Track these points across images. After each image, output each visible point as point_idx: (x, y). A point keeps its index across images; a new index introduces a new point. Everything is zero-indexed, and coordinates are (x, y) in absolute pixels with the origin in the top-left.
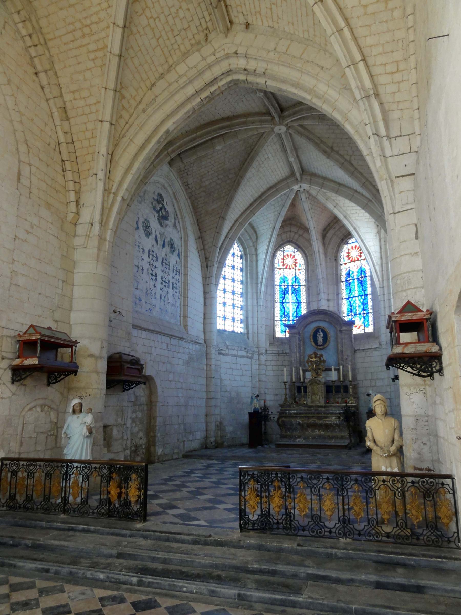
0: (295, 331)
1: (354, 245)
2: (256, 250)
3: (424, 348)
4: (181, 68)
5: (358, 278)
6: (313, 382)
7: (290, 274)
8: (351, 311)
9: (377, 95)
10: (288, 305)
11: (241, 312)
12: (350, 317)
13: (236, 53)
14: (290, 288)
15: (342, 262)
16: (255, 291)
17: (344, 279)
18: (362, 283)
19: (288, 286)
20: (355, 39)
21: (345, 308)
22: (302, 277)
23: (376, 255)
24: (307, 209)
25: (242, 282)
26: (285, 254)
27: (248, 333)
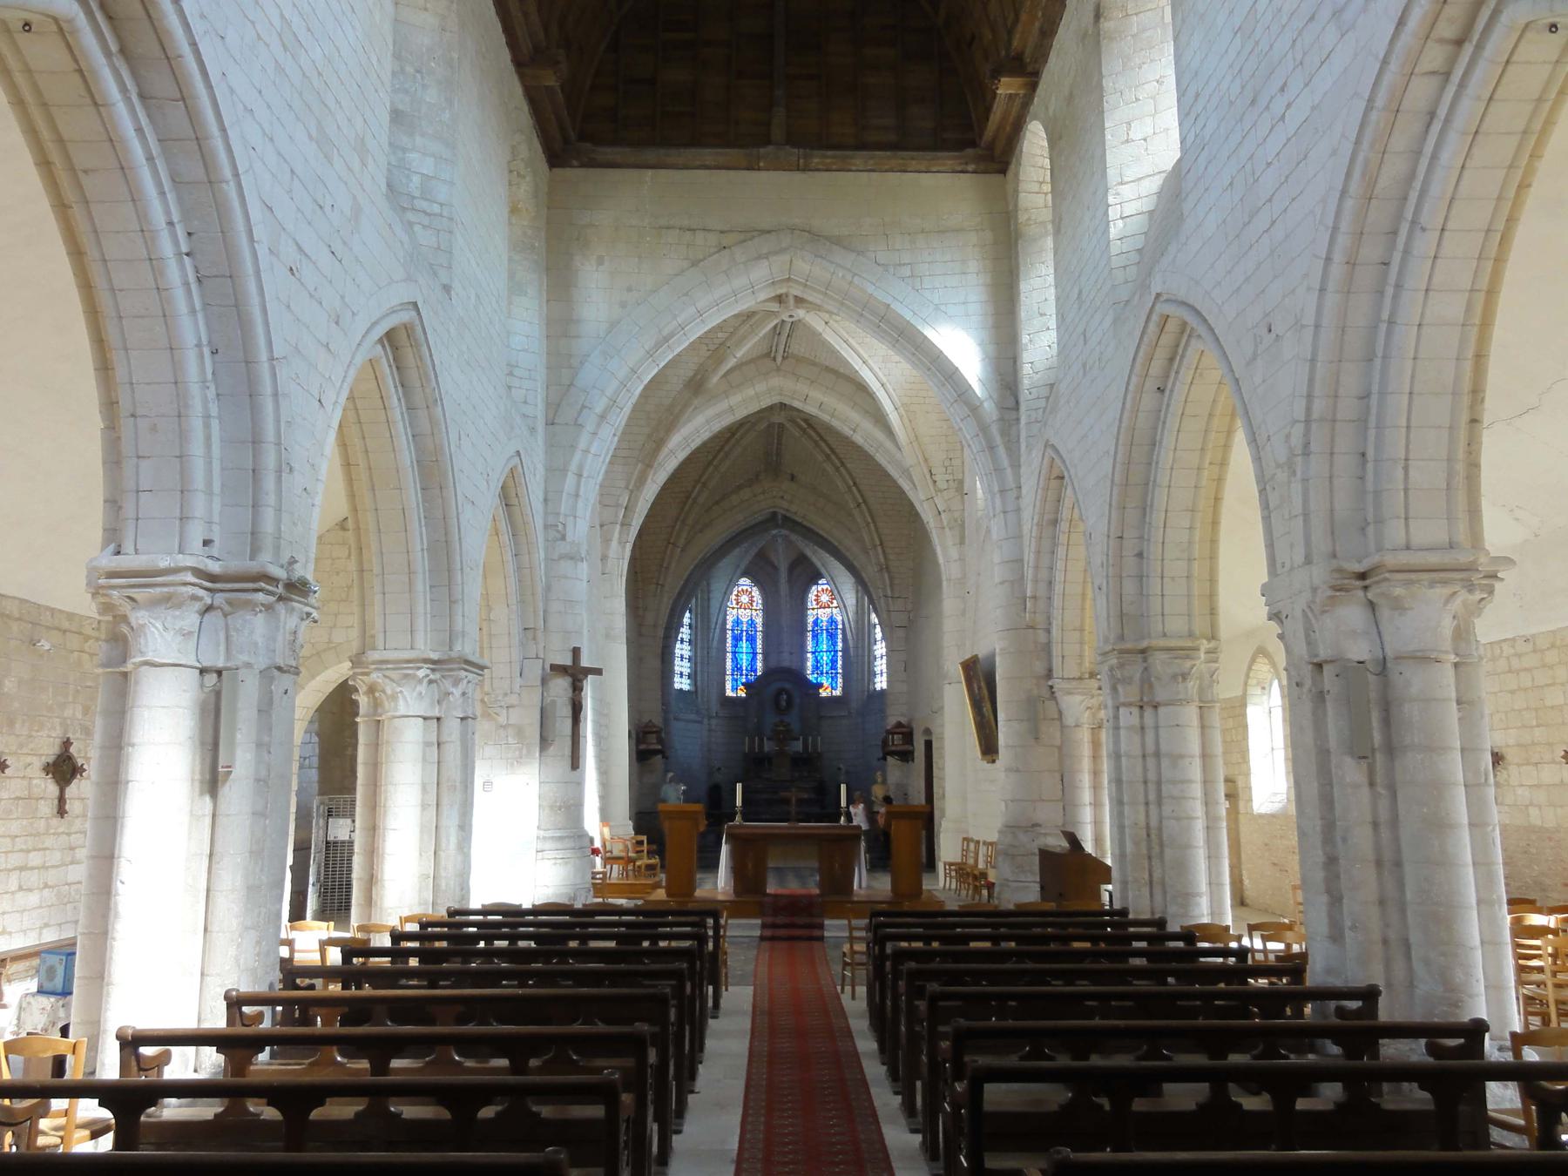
1: (825, 587)
2: (708, 585)
3: (906, 747)
4: (735, 499)
7: (745, 615)
8: (817, 668)
9: (887, 568)
11: (689, 665)
13: (782, 497)
14: (744, 634)
17: (810, 628)
18: (832, 636)
19: (742, 631)
21: (809, 664)
22: (759, 621)
25: (690, 625)
27: (696, 691)
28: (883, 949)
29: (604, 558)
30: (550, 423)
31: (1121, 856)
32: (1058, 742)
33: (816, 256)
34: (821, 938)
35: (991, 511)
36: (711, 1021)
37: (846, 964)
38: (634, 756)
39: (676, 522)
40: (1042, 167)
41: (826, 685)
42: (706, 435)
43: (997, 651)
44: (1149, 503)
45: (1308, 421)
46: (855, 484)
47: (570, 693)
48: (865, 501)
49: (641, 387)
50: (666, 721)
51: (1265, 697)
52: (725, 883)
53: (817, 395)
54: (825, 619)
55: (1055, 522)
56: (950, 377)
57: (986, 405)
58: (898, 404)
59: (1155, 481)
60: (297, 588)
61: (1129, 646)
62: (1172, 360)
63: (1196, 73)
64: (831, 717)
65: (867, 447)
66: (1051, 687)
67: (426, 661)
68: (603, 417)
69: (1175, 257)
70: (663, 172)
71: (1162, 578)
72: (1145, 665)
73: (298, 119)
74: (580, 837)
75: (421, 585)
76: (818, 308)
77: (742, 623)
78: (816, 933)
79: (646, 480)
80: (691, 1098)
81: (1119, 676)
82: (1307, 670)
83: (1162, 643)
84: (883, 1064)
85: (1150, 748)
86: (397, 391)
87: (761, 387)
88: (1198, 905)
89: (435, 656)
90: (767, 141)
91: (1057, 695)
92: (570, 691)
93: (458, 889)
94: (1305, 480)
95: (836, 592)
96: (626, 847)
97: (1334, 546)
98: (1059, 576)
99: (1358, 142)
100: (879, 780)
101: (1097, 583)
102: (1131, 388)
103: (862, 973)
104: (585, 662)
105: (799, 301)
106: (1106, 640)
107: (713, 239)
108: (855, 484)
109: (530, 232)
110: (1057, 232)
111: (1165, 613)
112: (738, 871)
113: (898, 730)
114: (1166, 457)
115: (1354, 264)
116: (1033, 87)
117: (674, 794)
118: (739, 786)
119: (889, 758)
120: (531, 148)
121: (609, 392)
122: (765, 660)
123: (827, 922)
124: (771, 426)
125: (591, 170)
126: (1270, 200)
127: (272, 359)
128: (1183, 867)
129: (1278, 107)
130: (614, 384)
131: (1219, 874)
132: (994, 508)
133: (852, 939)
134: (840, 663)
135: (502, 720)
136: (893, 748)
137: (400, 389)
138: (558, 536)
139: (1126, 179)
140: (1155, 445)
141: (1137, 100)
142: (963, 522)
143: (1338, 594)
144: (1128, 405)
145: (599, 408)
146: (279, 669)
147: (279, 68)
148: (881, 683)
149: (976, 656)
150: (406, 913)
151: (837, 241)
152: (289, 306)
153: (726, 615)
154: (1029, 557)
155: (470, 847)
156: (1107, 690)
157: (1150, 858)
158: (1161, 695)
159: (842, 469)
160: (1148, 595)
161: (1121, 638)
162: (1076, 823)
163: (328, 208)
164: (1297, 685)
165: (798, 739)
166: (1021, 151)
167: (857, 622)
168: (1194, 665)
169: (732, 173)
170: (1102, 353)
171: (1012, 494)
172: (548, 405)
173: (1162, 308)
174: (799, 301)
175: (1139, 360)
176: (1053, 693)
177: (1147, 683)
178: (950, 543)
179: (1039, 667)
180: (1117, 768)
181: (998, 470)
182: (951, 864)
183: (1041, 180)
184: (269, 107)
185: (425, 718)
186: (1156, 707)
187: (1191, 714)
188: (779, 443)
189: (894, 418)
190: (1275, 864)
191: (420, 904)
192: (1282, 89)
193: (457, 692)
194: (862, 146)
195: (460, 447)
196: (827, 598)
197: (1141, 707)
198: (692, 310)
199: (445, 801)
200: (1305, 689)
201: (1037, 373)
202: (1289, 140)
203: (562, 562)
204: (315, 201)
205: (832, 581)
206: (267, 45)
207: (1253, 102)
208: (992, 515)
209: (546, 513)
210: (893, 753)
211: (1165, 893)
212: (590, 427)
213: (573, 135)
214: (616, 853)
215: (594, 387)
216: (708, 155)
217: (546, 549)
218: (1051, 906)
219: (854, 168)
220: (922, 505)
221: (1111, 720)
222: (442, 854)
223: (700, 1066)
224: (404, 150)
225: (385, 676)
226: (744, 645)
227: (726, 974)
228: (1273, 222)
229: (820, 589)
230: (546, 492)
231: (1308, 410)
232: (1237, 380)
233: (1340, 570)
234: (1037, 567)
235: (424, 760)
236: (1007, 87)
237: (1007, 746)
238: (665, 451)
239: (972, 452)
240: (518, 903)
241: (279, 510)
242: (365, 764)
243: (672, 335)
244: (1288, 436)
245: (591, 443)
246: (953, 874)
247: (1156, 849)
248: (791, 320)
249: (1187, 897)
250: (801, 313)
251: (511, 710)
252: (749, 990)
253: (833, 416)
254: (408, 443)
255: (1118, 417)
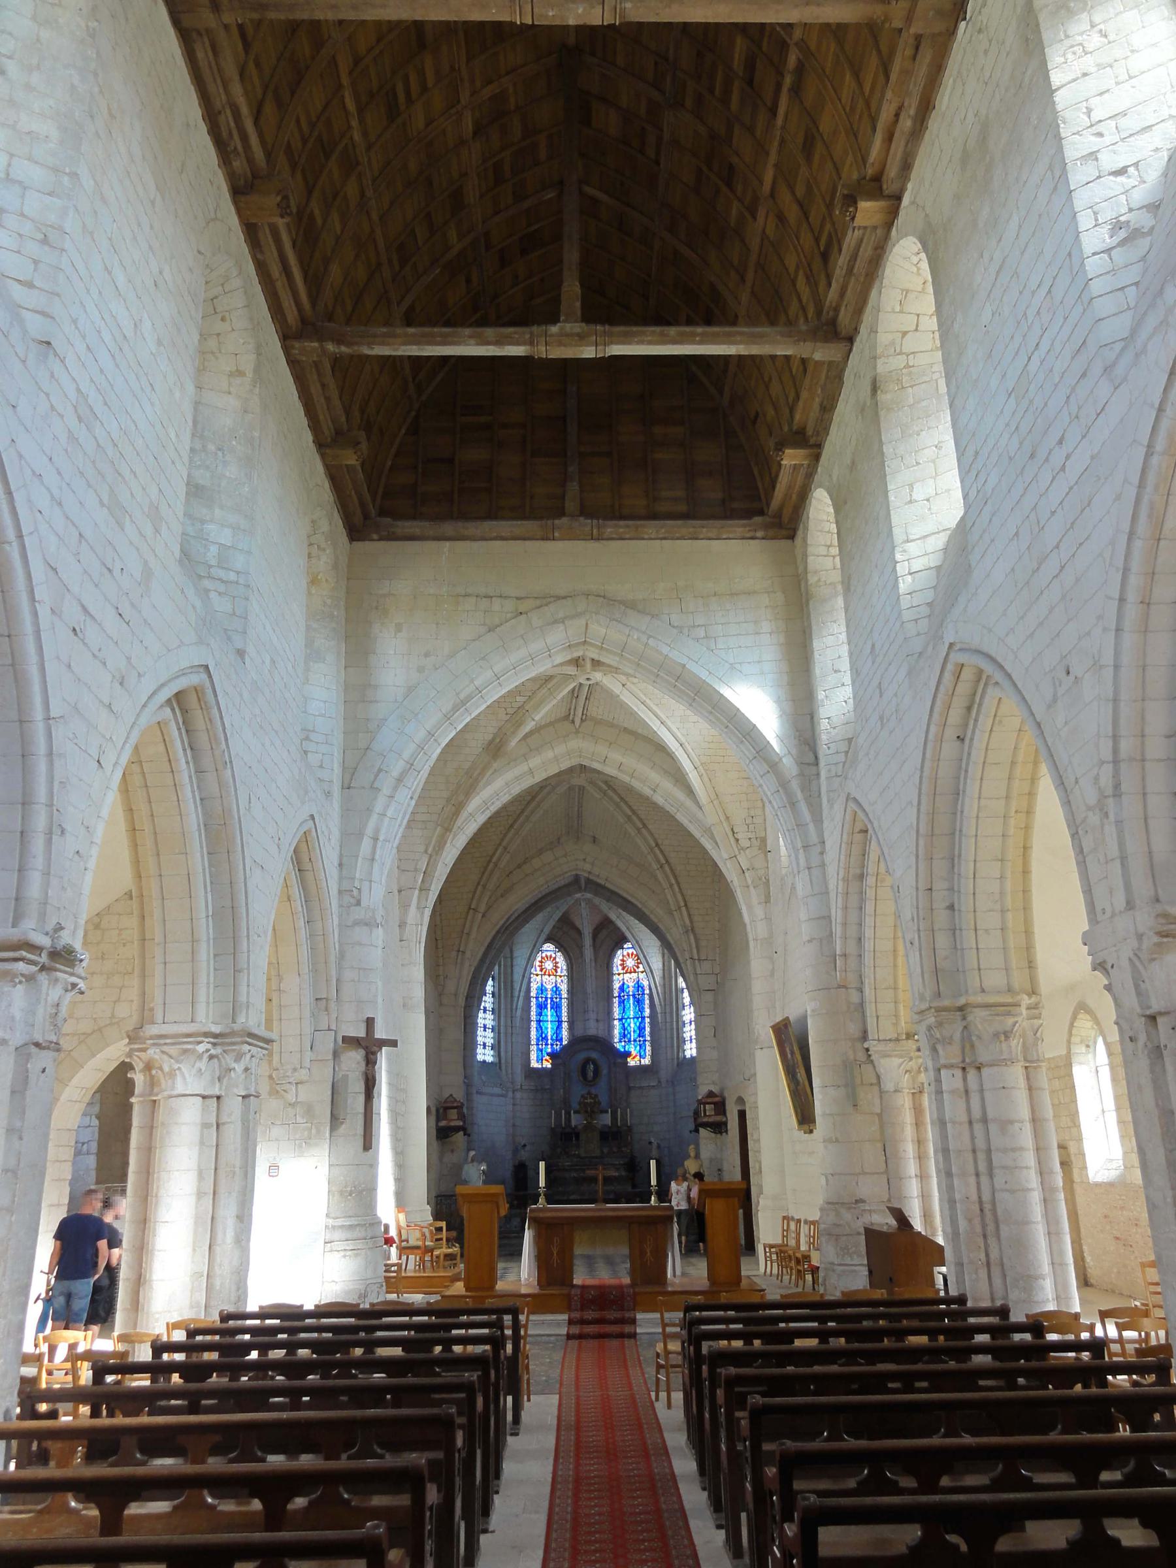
0: (560, 1061)
1: (630, 951)
2: (512, 951)
3: (719, 1118)
4: (536, 863)
5: (634, 995)
6: (589, 1127)
7: (549, 982)
8: (625, 1036)
9: (692, 929)
10: (545, 1024)
11: (492, 1035)
12: (623, 1044)
13: (584, 860)
14: (549, 1001)
15: (615, 971)
16: (509, 1006)
17: (616, 994)
18: (639, 1002)
19: (546, 998)
20: (680, 889)
21: (617, 1032)
22: (564, 987)
23: (658, 974)
24: (584, 915)
25: (493, 994)
26: (544, 955)
28: (698, 1349)
29: (403, 925)
30: (346, 787)
31: (954, 1235)
32: (879, 1111)
33: (612, 620)
34: (633, 1335)
35: (795, 866)
36: (510, 1439)
37: (659, 1366)
38: (434, 1132)
39: (477, 888)
40: (829, 532)
41: (634, 1053)
42: (505, 798)
43: (809, 1013)
44: (956, 853)
45: (1116, 762)
46: (657, 845)
47: (362, 1066)
48: (667, 861)
49: (439, 751)
50: (468, 1095)
51: (1090, 1056)
52: (529, 1274)
53: (616, 756)
54: (631, 984)
55: (861, 877)
56: (748, 734)
57: (784, 760)
58: (698, 764)
59: (961, 831)
60: (62, 956)
61: (946, 1003)
62: (969, 709)
63: (974, 435)
64: (640, 1088)
65: (668, 807)
66: (867, 1050)
67: (206, 1034)
68: (400, 780)
69: (967, 606)
70: (460, 545)
71: (976, 930)
72: (964, 1023)
73: (89, 486)
74: (372, 1225)
75: (204, 953)
76: (616, 670)
77: (546, 990)
78: (627, 1329)
79: (445, 844)
80: (483, 1538)
81: (938, 1036)
82: (1140, 1024)
83: (980, 999)
84: (704, 1489)
85: (977, 1113)
86: (186, 755)
87: (560, 749)
88: (1043, 1288)
89: (216, 1029)
90: (561, 513)
91: (873, 1058)
92: (363, 1064)
93: (234, 1288)
94: (1119, 823)
95: (641, 956)
96: (424, 1235)
97: (1156, 891)
98: (869, 933)
99: (1141, 485)
100: (692, 1154)
101: (908, 937)
102: (931, 736)
103: (678, 1379)
104: (380, 1034)
105: (596, 663)
106: (922, 998)
107: (509, 605)
108: (657, 845)
109: (329, 601)
110: (847, 589)
111: (981, 967)
112: (542, 1259)
113: (709, 1100)
114: (970, 806)
115: (1149, 604)
116: (817, 457)
117: (475, 1174)
118: (542, 1165)
119: (701, 1130)
120: (331, 522)
121: (406, 755)
122: (571, 1028)
123: (639, 1316)
124: (571, 788)
125: (389, 542)
126: (1057, 547)
127: (48, 718)
128: (1022, 1245)
129: (1058, 458)
130: (412, 747)
131: (1062, 1253)
132: (798, 864)
133: (666, 1337)
134: (648, 1029)
135: (291, 1097)
136: (705, 1120)
137: (189, 751)
138: (353, 901)
139: (911, 537)
140: (958, 794)
141: (918, 464)
142: (768, 881)
143: (1165, 940)
144: (928, 755)
145: (396, 769)
146: (37, 1045)
147: (72, 438)
148: (690, 1050)
149: (788, 1018)
150: (175, 1318)
151: (631, 605)
152: (69, 666)
153: (529, 982)
154: (837, 914)
155: (248, 1240)
156: (926, 1051)
157: (985, 1236)
158: (983, 1056)
159: (644, 831)
160: (963, 949)
161: (939, 995)
162: (902, 1198)
163: (117, 572)
164: (1131, 1039)
165: (607, 1112)
166: (808, 518)
167: (664, 985)
168: (1016, 1022)
169: (528, 543)
170: (898, 705)
171: (818, 849)
172: (344, 769)
173: (957, 657)
174: (596, 663)
175: (937, 710)
176: (870, 1056)
177: (968, 1042)
178: (755, 900)
179: (853, 1029)
180: (943, 1136)
181: (800, 825)
182: (771, 1246)
183: (829, 543)
184: (59, 473)
185: (204, 1097)
186: (979, 1069)
187: (1016, 1074)
188: (580, 806)
189: (693, 777)
190: (1117, 1238)
191: (192, 1307)
192: (1060, 442)
193: (239, 1067)
194: (654, 516)
195: (249, 810)
196: (633, 963)
197: (964, 1069)
198: (489, 674)
199: (222, 1190)
200: (1141, 1043)
201: (834, 728)
202: (1071, 488)
203: (357, 929)
204: (104, 564)
205: (638, 945)
206: (62, 416)
207: (1032, 456)
208: (796, 872)
209: (341, 878)
210: (705, 1125)
211: (1004, 1276)
212: (386, 791)
213: (373, 513)
214: (412, 1242)
215: (391, 750)
216: (504, 526)
217: (340, 916)
218: (880, 1294)
219: (646, 536)
220: (725, 864)
221: (933, 1084)
222: (218, 1250)
223: (495, 1497)
224: (203, 522)
225: (163, 1052)
226: (549, 1013)
227: (528, 1380)
228: (1063, 567)
229: (625, 953)
230: (341, 856)
231: (1115, 751)
232: (1039, 725)
233: (1165, 915)
234: (845, 924)
235: (202, 1143)
236: (791, 458)
237: (824, 1115)
238: (464, 814)
239: (773, 807)
240: (298, 1304)
241: (47, 874)
242: (138, 1148)
243: (469, 698)
244: (1097, 778)
245: (387, 807)
246: (774, 1257)
247: (991, 1228)
248: (589, 683)
249: (1029, 1280)
250: (597, 676)
251: (299, 1086)
252: (555, 1399)
253: (632, 776)
254: (196, 807)
255: (919, 767)
